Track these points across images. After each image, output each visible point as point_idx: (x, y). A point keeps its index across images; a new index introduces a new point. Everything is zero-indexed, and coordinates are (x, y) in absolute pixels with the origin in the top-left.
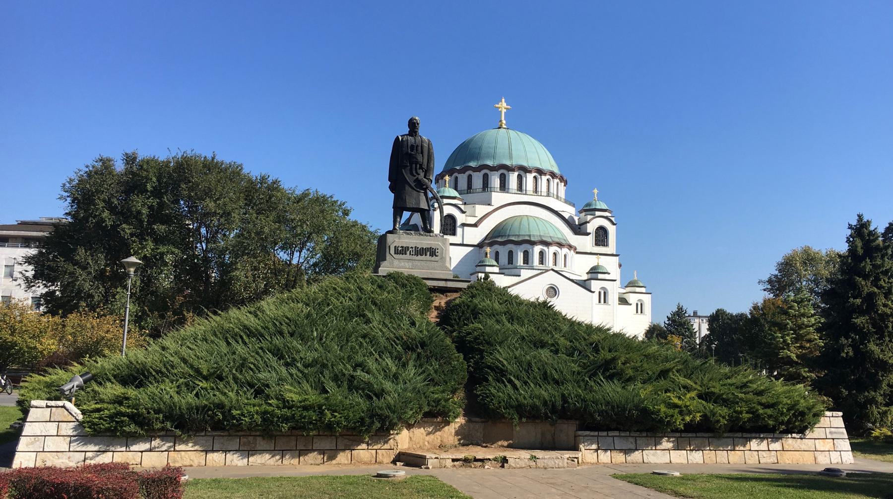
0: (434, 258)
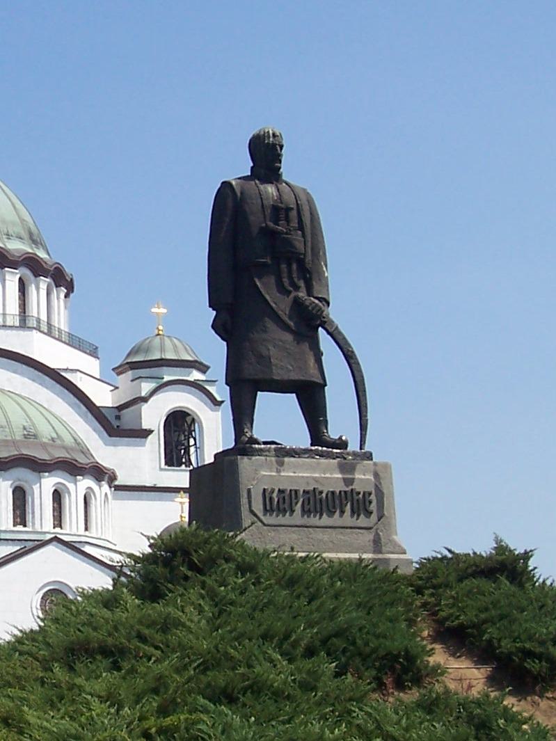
0: (363, 521)
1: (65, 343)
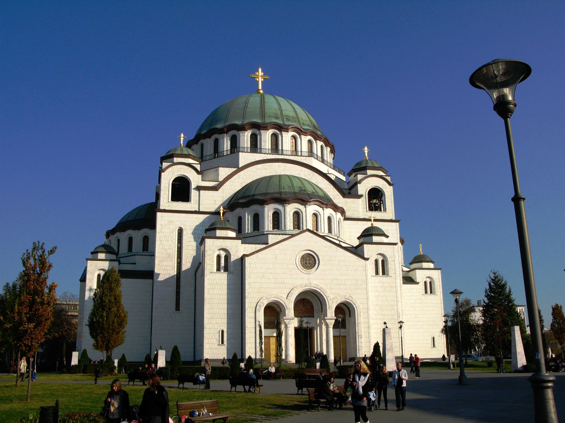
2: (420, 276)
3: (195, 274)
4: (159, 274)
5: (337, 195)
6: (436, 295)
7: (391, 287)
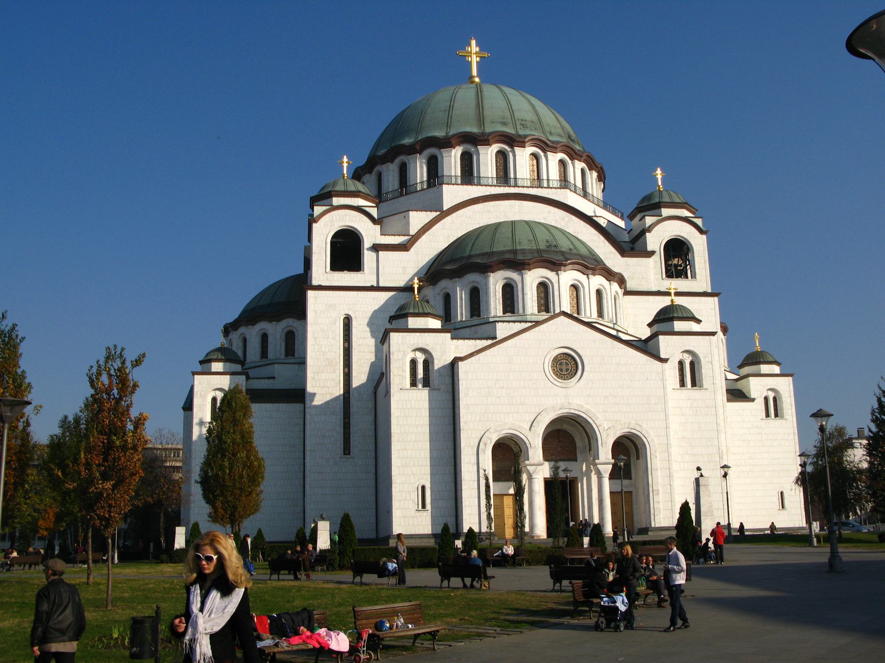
1: (595, 204)
2: (757, 387)
3: (375, 393)
4: (314, 394)
5: (611, 253)
6: (785, 419)
7: (707, 407)
